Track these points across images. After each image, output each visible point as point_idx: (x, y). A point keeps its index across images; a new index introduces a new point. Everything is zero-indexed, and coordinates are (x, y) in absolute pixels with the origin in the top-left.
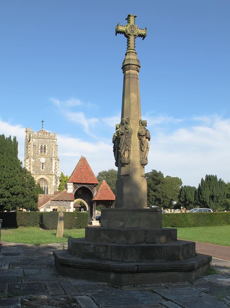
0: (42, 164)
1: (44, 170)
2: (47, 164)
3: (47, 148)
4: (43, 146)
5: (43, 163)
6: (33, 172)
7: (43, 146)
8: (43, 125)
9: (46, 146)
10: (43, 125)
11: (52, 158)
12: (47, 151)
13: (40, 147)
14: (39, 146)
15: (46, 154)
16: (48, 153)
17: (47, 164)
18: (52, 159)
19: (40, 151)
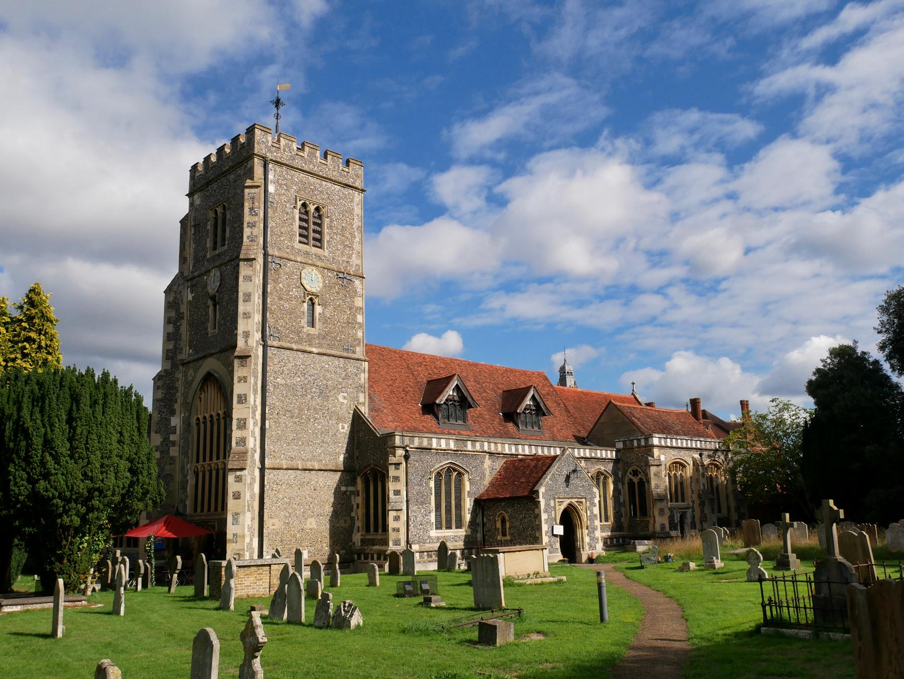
0: (210, 303)
3: (228, 216)
5: (213, 298)
15: (226, 247)
19: (209, 244)
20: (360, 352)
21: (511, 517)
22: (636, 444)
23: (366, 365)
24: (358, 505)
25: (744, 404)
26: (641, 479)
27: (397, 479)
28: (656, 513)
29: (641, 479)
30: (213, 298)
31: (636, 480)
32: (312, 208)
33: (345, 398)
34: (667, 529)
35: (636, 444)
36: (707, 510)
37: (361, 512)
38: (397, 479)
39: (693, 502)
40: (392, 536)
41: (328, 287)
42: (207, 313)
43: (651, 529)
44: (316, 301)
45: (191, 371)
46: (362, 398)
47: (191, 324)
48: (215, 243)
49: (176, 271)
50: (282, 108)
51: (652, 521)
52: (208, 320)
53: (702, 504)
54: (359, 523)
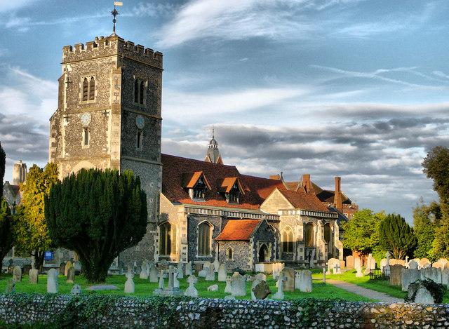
0: (84, 130)
1: (88, 146)
2: (96, 130)
4: (89, 79)
5: (86, 129)
6: (67, 154)
7: (89, 79)
8: (114, 21)
9: (95, 77)
10: (114, 21)
11: (108, 111)
13: (81, 85)
14: (79, 81)
15: (94, 101)
16: (99, 98)
17: (96, 130)
19: (81, 96)
20: (159, 159)
23: (161, 167)
24: (157, 241)
26: (291, 232)
28: (298, 251)
29: (291, 232)
30: (86, 129)
31: (288, 233)
34: (303, 259)
37: (158, 244)
41: (146, 126)
42: (81, 135)
43: (294, 259)
44: (142, 133)
45: (68, 165)
47: (67, 139)
48: (85, 96)
50: (117, 16)
51: (295, 254)
52: (82, 139)
54: (157, 250)
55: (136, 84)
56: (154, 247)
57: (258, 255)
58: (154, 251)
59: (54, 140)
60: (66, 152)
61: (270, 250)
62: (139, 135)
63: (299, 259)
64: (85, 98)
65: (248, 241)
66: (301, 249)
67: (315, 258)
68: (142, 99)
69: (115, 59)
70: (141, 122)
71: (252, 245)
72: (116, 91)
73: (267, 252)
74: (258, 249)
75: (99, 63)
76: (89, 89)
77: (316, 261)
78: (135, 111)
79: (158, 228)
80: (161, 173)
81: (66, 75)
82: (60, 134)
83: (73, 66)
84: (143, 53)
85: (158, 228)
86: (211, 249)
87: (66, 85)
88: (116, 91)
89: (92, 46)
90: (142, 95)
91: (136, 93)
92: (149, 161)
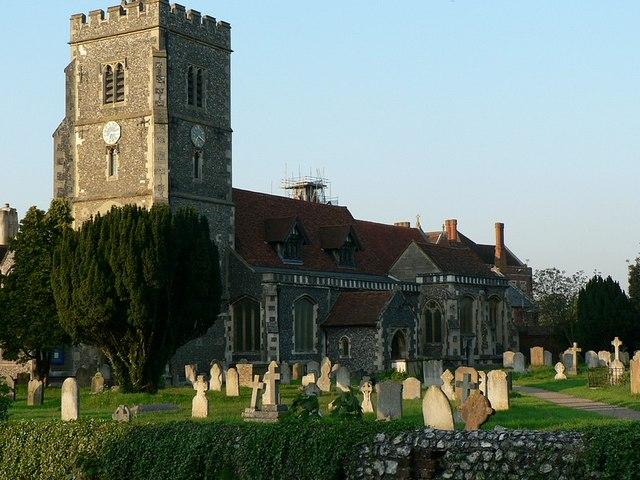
2: (128, 150)
3: (126, 75)
5: (112, 149)
6: (83, 191)
11: (146, 119)
12: (126, 90)
15: (124, 103)
16: (132, 97)
17: (128, 150)
18: (143, 122)
20: (229, 196)
21: (353, 341)
22: (435, 281)
23: (233, 209)
24: (230, 329)
25: (501, 227)
27: (271, 308)
28: (451, 340)
31: (433, 311)
32: (195, 71)
33: (220, 238)
35: (435, 281)
36: (489, 339)
38: (271, 308)
39: (477, 331)
40: (271, 353)
45: (85, 209)
46: (231, 238)
49: (60, 115)
51: (445, 346)
53: (485, 333)
54: (230, 343)
55: (190, 75)
56: (225, 339)
57: (390, 348)
58: (225, 345)
59: (61, 169)
60: (82, 188)
61: (408, 340)
62: (197, 157)
63: (451, 353)
64: (107, 99)
65: (374, 327)
66: (455, 338)
67: (476, 353)
68: (199, 99)
69: (155, 33)
70: (199, 137)
71: (380, 332)
72: (159, 86)
73: (404, 343)
74: (390, 339)
75: (130, 39)
76: (114, 83)
77: (477, 357)
78: (190, 118)
79: (231, 308)
80: (232, 219)
81: (78, 63)
82: (70, 159)
83: (88, 46)
84: (199, 22)
85: (231, 308)
86: (315, 339)
87: (78, 79)
88: (159, 86)
89: (118, 13)
90: (199, 92)
91: (190, 89)
92: (215, 200)
